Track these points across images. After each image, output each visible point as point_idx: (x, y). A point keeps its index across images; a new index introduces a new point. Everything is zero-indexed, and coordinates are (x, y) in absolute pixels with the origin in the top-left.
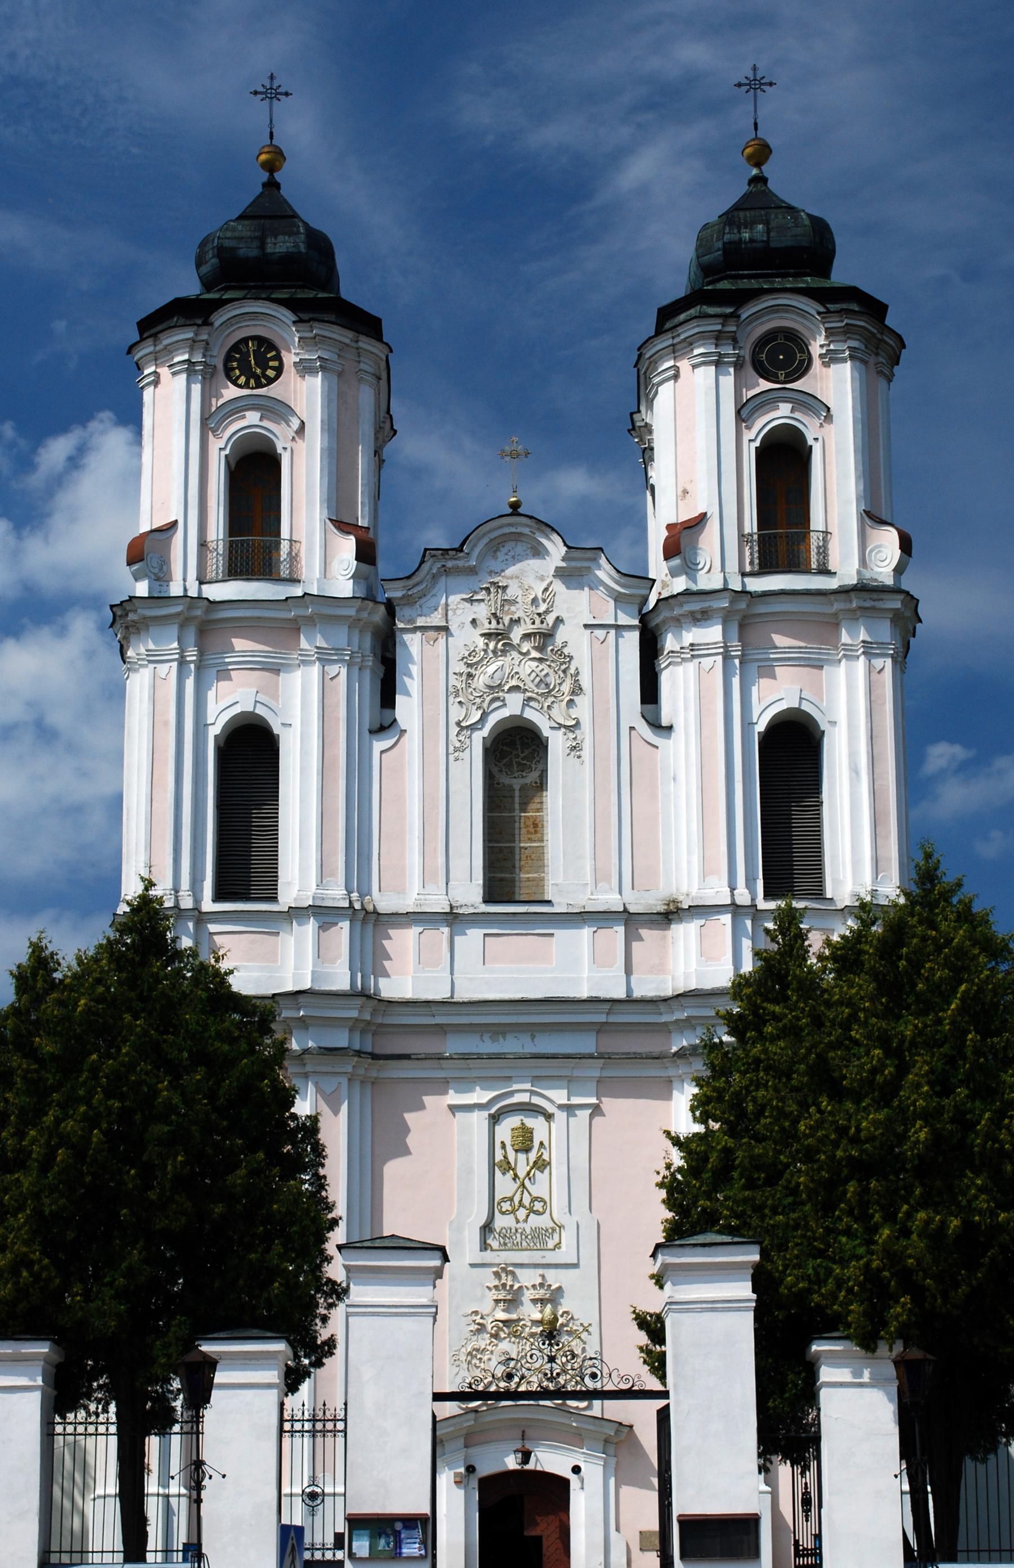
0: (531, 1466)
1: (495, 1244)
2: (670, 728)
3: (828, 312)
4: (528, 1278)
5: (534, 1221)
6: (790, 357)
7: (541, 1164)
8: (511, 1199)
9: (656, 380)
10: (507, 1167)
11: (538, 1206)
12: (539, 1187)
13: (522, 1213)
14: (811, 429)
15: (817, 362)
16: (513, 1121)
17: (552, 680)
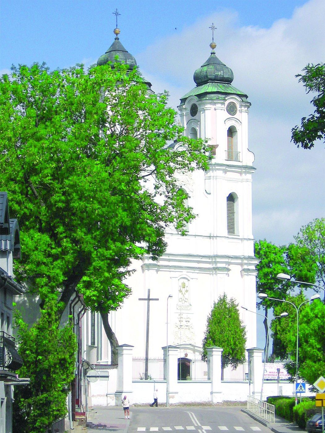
0: (187, 358)
1: (179, 309)
2: (210, 194)
3: (243, 101)
4: (184, 316)
5: (187, 304)
6: (233, 111)
7: (187, 291)
8: (181, 298)
9: (205, 109)
10: (180, 291)
11: (186, 300)
12: (187, 296)
13: (183, 302)
14: (238, 128)
15: (238, 111)
16: (182, 281)
17: (189, 180)
